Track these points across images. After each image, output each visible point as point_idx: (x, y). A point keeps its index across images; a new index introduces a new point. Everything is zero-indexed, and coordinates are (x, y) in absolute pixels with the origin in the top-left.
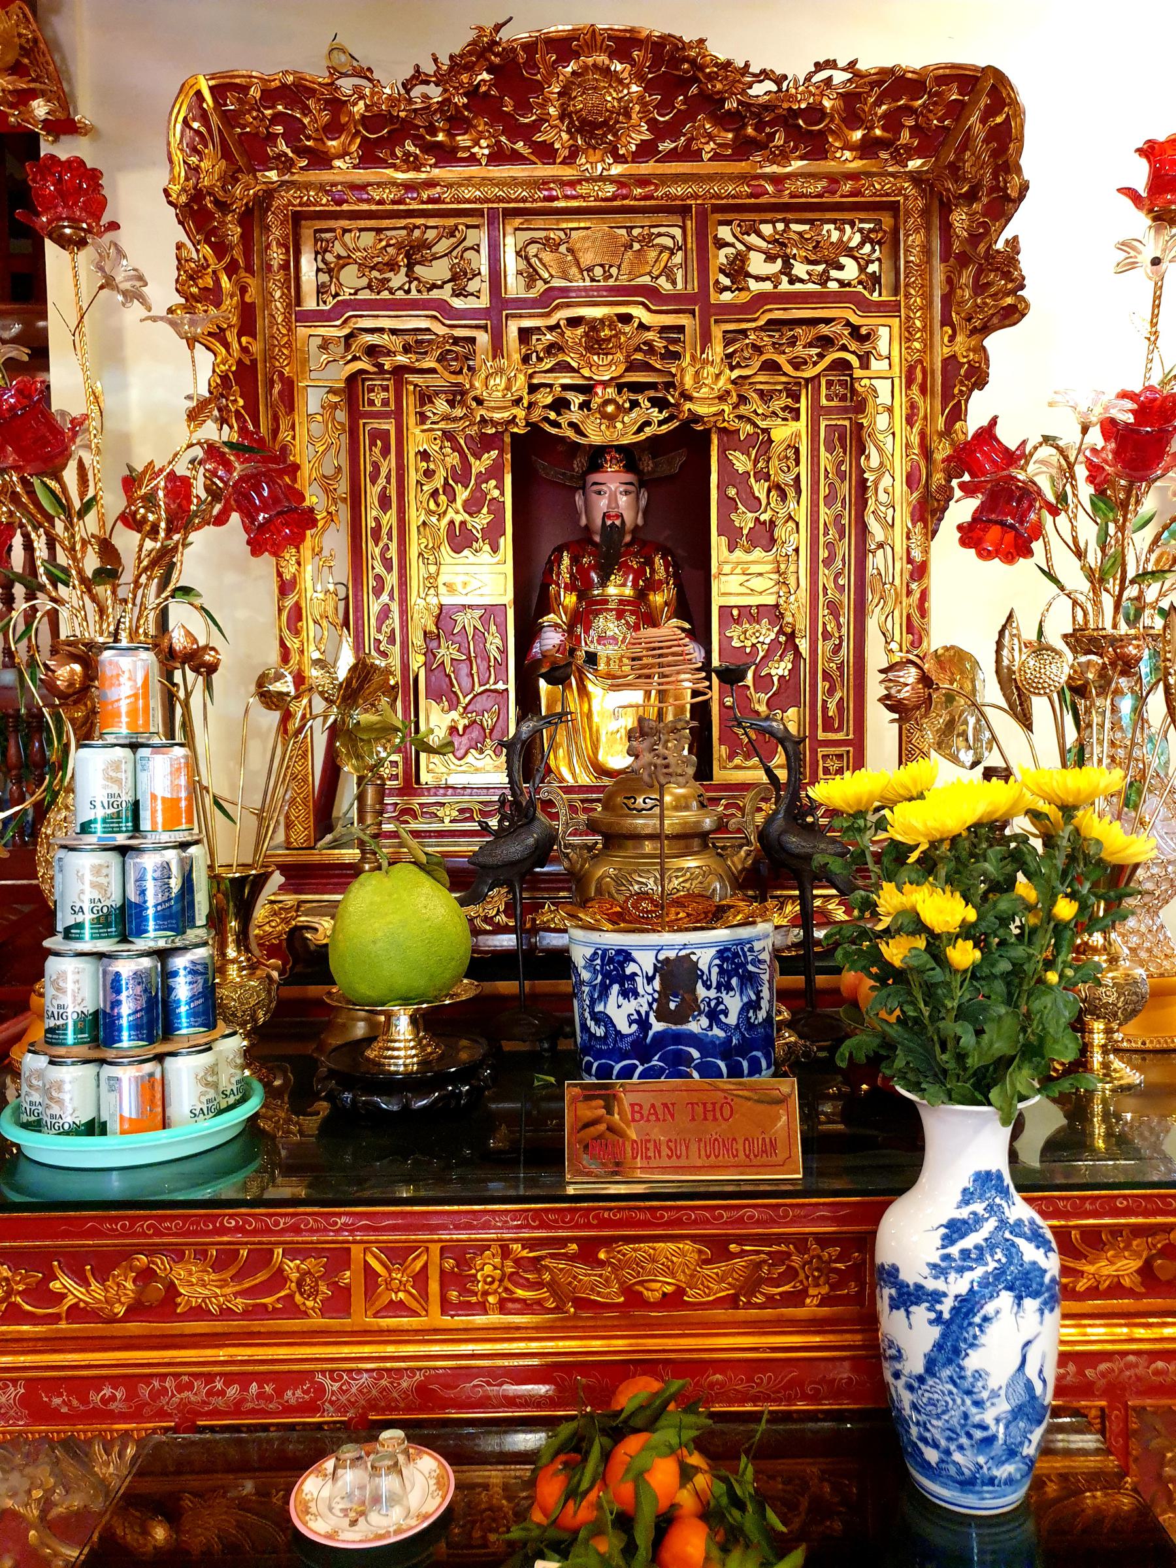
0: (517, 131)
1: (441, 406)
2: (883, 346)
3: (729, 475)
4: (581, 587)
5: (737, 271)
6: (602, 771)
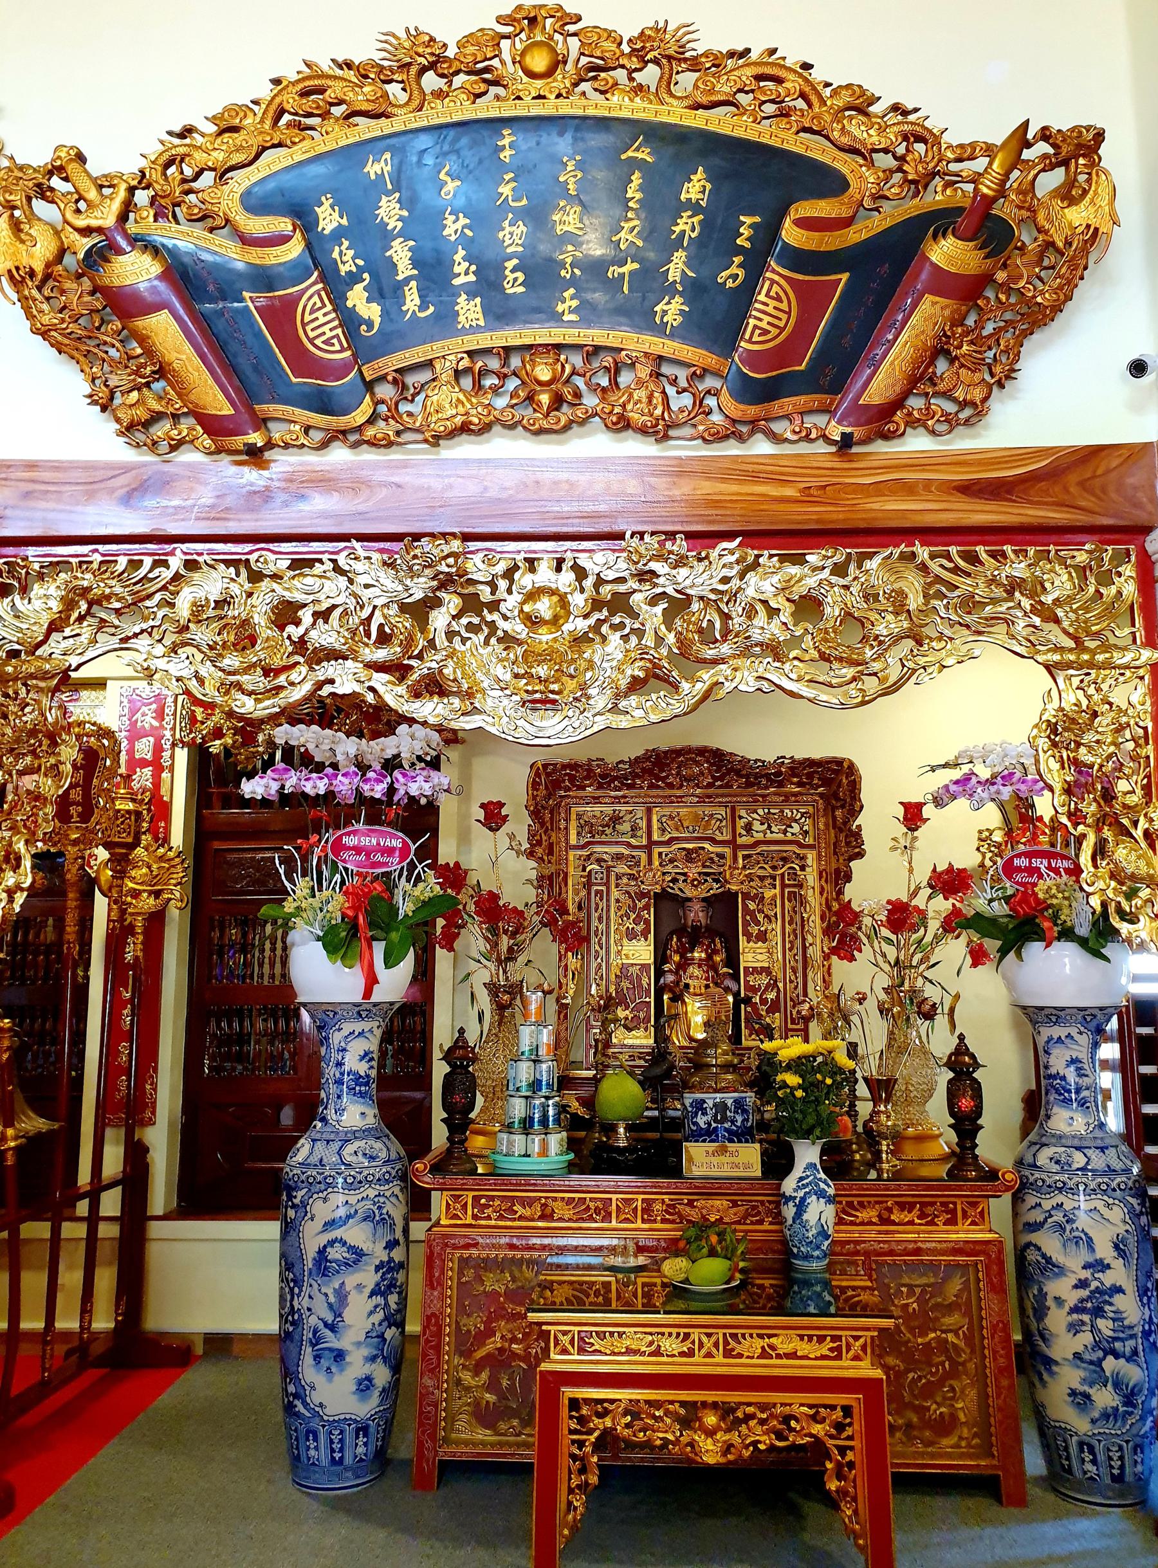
0: (658, 779)
1: (625, 880)
2: (809, 862)
3: (746, 910)
4: (682, 951)
5: (748, 828)
6: (692, 1039)
